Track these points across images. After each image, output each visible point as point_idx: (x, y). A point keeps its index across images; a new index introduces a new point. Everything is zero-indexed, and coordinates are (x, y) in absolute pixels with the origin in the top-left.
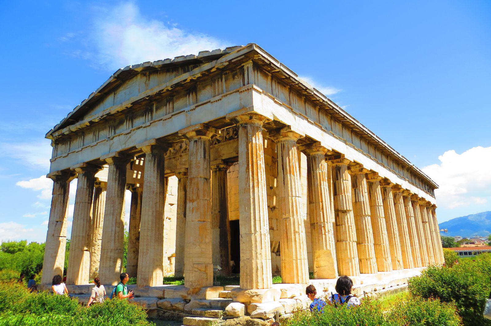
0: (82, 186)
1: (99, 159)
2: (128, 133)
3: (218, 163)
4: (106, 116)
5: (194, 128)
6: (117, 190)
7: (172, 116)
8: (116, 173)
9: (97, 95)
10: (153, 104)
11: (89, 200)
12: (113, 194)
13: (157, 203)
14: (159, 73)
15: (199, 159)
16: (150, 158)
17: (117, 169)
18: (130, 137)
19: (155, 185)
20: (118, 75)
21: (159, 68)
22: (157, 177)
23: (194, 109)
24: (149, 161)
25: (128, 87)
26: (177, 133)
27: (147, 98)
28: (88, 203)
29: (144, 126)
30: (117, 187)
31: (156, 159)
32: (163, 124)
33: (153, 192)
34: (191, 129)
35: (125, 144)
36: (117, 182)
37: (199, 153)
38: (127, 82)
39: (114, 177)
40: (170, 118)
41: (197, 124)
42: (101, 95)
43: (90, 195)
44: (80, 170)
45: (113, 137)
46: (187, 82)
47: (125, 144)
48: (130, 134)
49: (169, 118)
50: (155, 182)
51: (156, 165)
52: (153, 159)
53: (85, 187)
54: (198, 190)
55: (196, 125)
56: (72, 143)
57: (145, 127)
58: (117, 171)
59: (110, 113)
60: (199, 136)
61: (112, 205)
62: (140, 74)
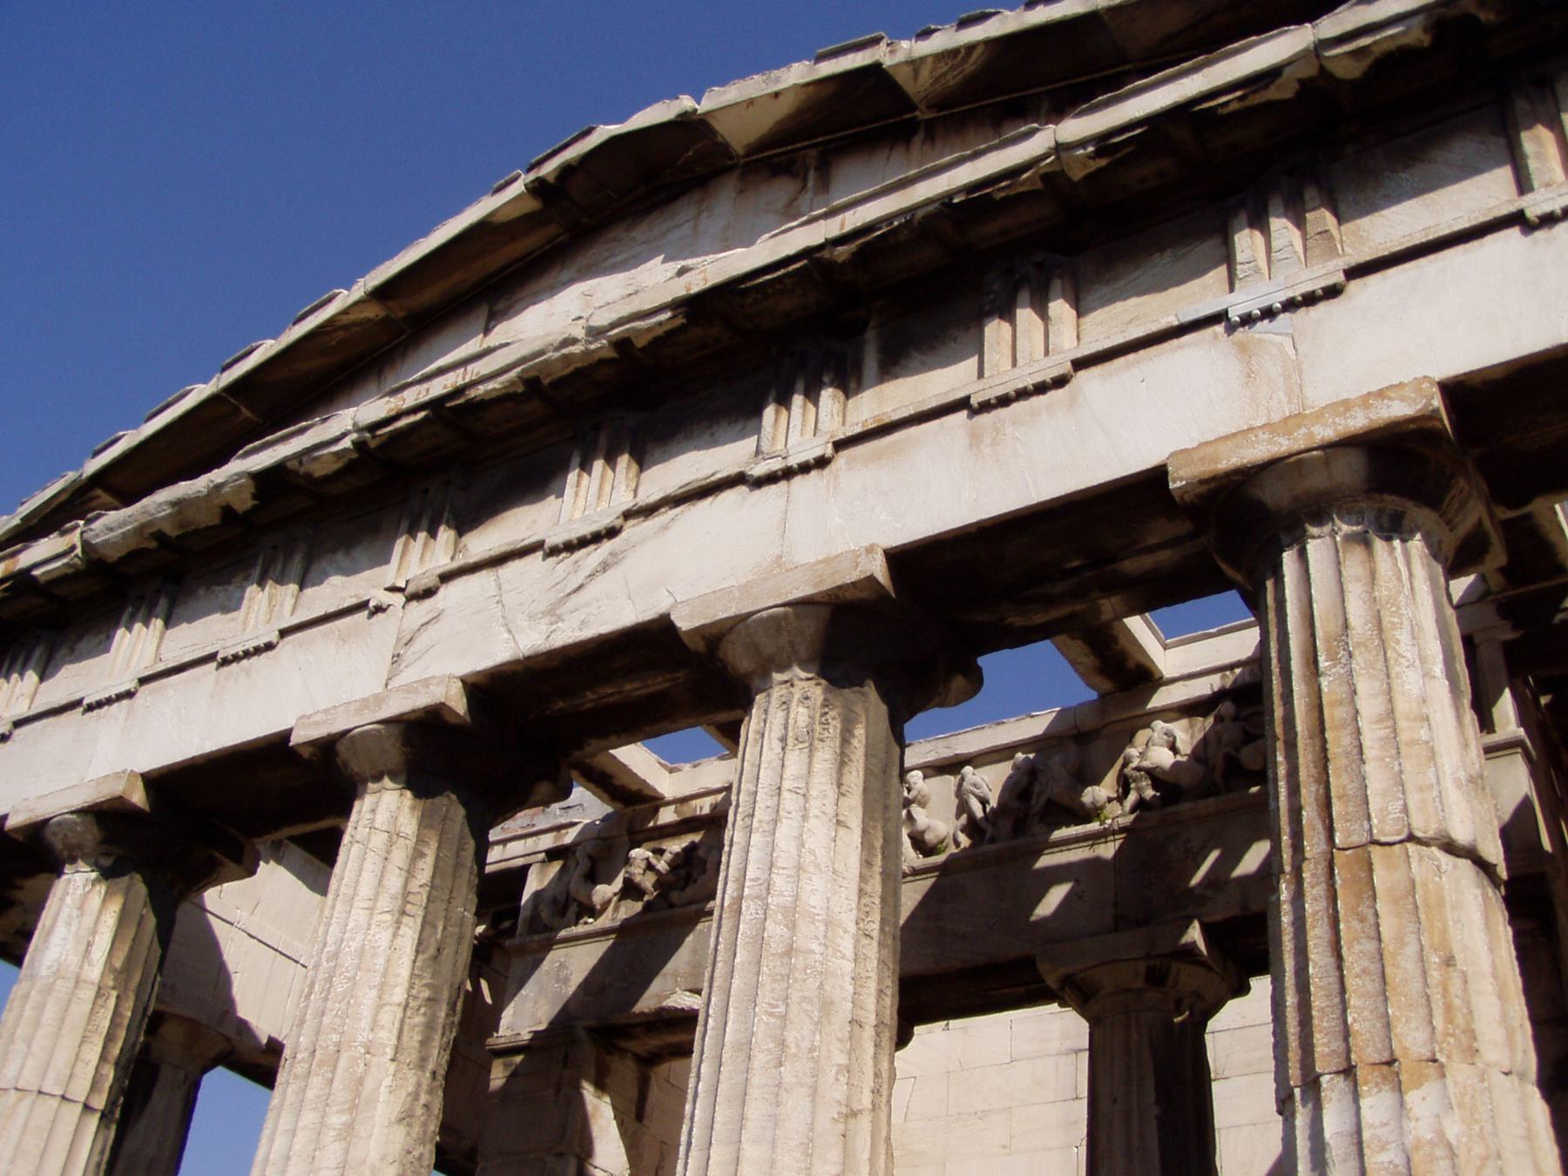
0: (74, 960)
1: (286, 735)
2: (596, 538)
4: (422, 415)
5: (1358, 422)
6: (399, 995)
7: (1081, 364)
8: (417, 854)
9: (352, 317)
10: (858, 329)
11: (95, 1086)
12: (365, 1023)
14: (918, 139)
15: (1409, 682)
16: (801, 715)
17: (425, 822)
18: (605, 567)
19: (847, 945)
20: (567, 171)
21: (929, 107)
22: (863, 878)
23: (1332, 292)
25: (619, 258)
26: (1158, 475)
27: (842, 252)
28: (87, 1108)
29: (759, 470)
30: (404, 971)
31: (860, 731)
32: (975, 438)
34: (1326, 432)
35: (553, 613)
36: (410, 932)
37: (1403, 636)
38: (618, 231)
39: (394, 882)
40: (1060, 382)
41: (1401, 385)
42: (385, 322)
43: (116, 1051)
44: (90, 834)
45: (446, 577)
46: (1273, 93)
47: (553, 613)
48: (607, 546)
49: (1041, 389)
50: (848, 919)
51: (855, 777)
52: (835, 726)
53: (95, 972)
54: (1449, 961)
55: (1381, 394)
56: (64, 651)
57: (771, 479)
58: (420, 840)
59: (459, 391)
60: (1391, 501)
61: (336, 1120)
62: (736, 174)
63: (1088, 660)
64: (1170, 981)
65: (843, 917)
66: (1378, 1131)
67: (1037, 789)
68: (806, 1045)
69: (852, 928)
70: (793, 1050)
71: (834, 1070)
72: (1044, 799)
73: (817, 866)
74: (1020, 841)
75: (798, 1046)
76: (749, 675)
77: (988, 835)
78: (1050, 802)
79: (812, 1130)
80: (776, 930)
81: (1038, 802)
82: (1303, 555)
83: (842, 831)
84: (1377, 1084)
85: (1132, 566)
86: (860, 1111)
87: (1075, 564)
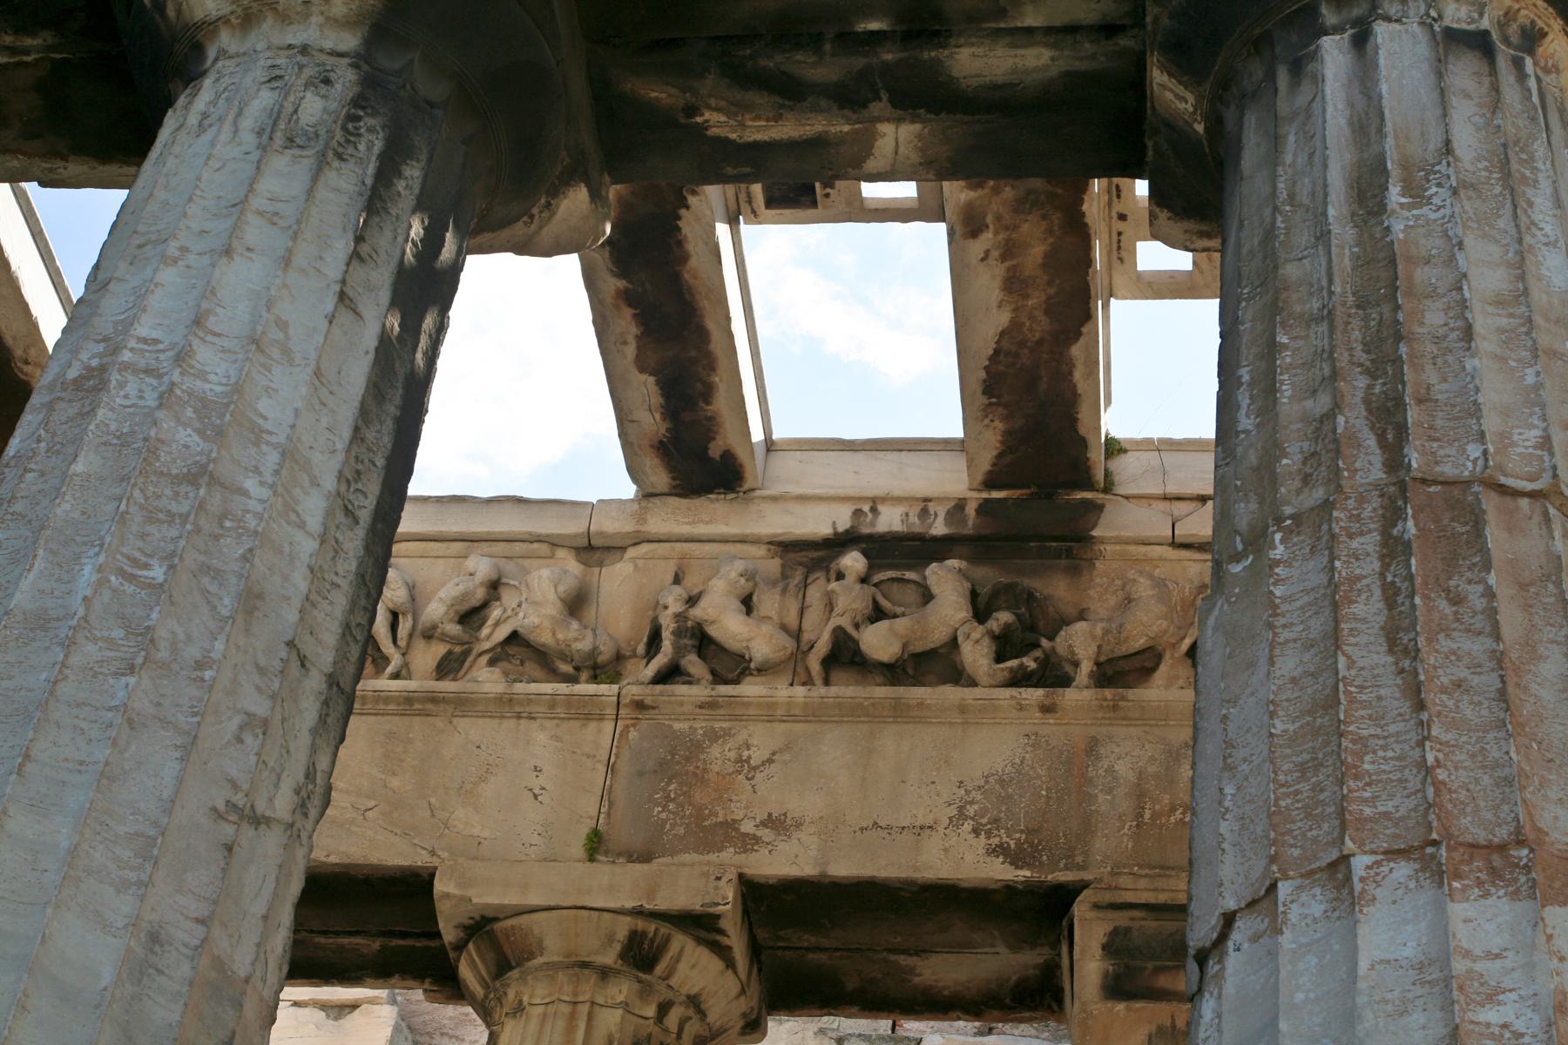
3: (681, 894)
13: (257, 820)
16: (313, 108)
19: (314, 507)
24: (280, 133)
33: (251, 601)
52: (372, 143)
63: (652, 423)
64: (660, 969)
65: (317, 457)
66: (1478, 967)
67: (495, 613)
68: (193, 652)
69: (329, 483)
70: (163, 654)
71: (237, 720)
72: (502, 633)
73: (287, 352)
74: (448, 686)
75: (174, 649)
76: (210, 27)
77: (390, 670)
78: (514, 637)
79: (169, 812)
80: (183, 438)
81: (493, 633)
82: (1361, 40)
83: (345, 317)
84: (1479, 883)
85: (975, 62)
86: (268, 821)
87: (874, 26)
